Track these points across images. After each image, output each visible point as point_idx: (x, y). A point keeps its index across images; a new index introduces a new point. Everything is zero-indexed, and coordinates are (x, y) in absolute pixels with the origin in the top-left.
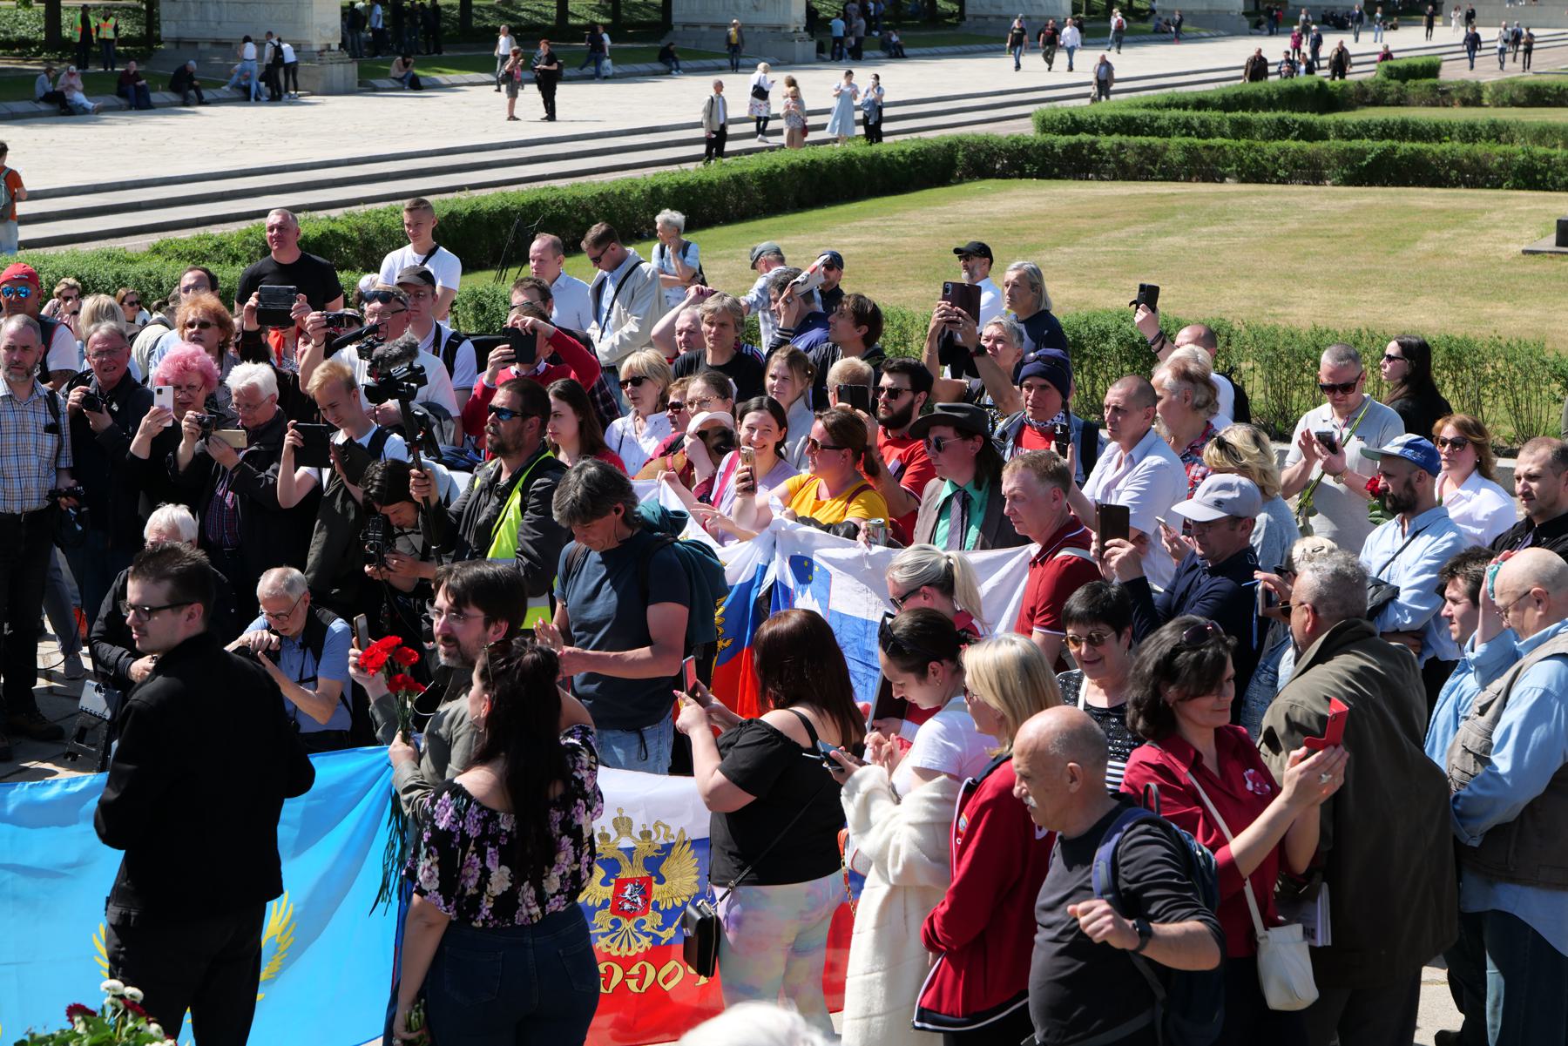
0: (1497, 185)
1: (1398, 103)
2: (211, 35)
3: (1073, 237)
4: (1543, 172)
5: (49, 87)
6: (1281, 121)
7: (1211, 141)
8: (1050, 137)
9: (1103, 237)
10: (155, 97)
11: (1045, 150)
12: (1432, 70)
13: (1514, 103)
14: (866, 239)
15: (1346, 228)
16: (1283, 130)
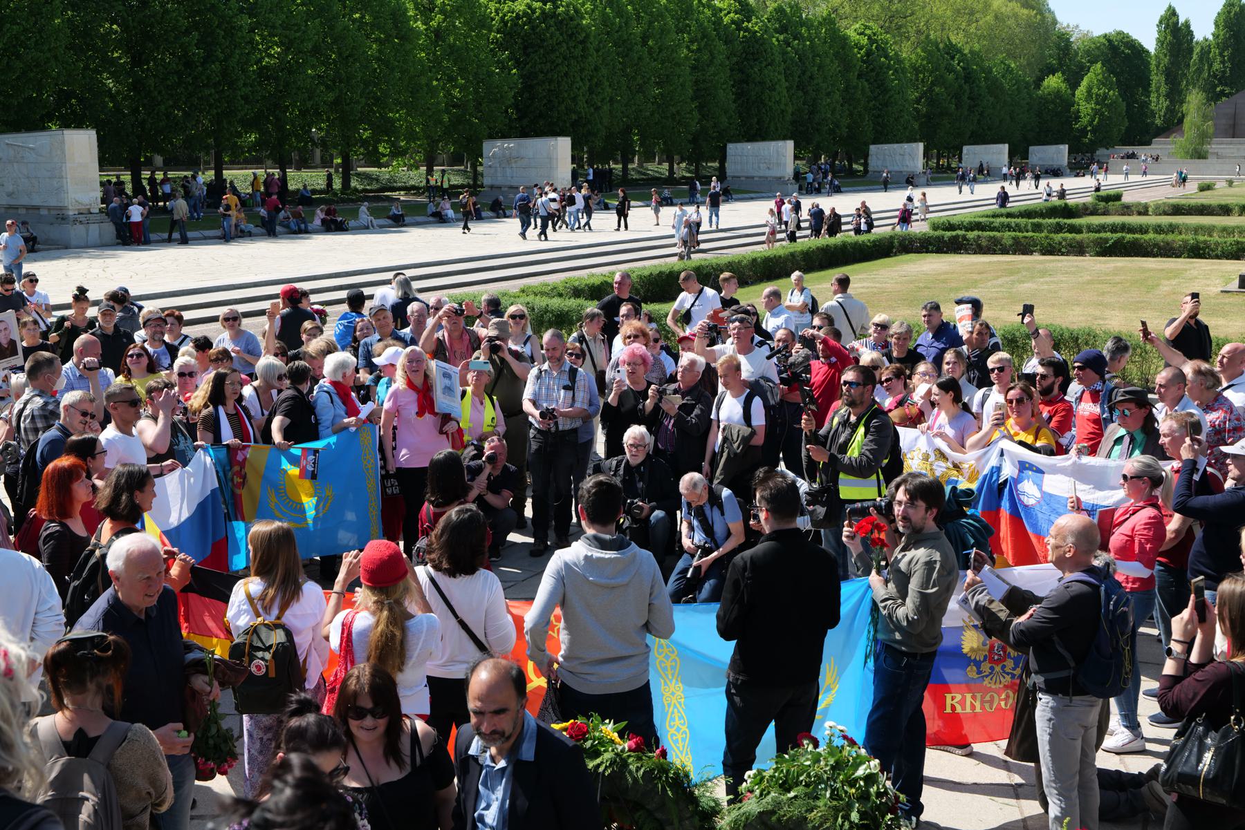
0: (1179, 257)
1: (1104, 214)
2: (508, 183)
4: (1204, 249)
5: (434, 209)
6: (1058, 224)
7: (1026, 234)
8: (939, 233)
9: (989, 284)
10: (484, 214)
11: (940, 239)
12: (1118, 197)
13: (1165, 213)
14: (865, 284)
15: (1117, 279)
16: (1059, 229)
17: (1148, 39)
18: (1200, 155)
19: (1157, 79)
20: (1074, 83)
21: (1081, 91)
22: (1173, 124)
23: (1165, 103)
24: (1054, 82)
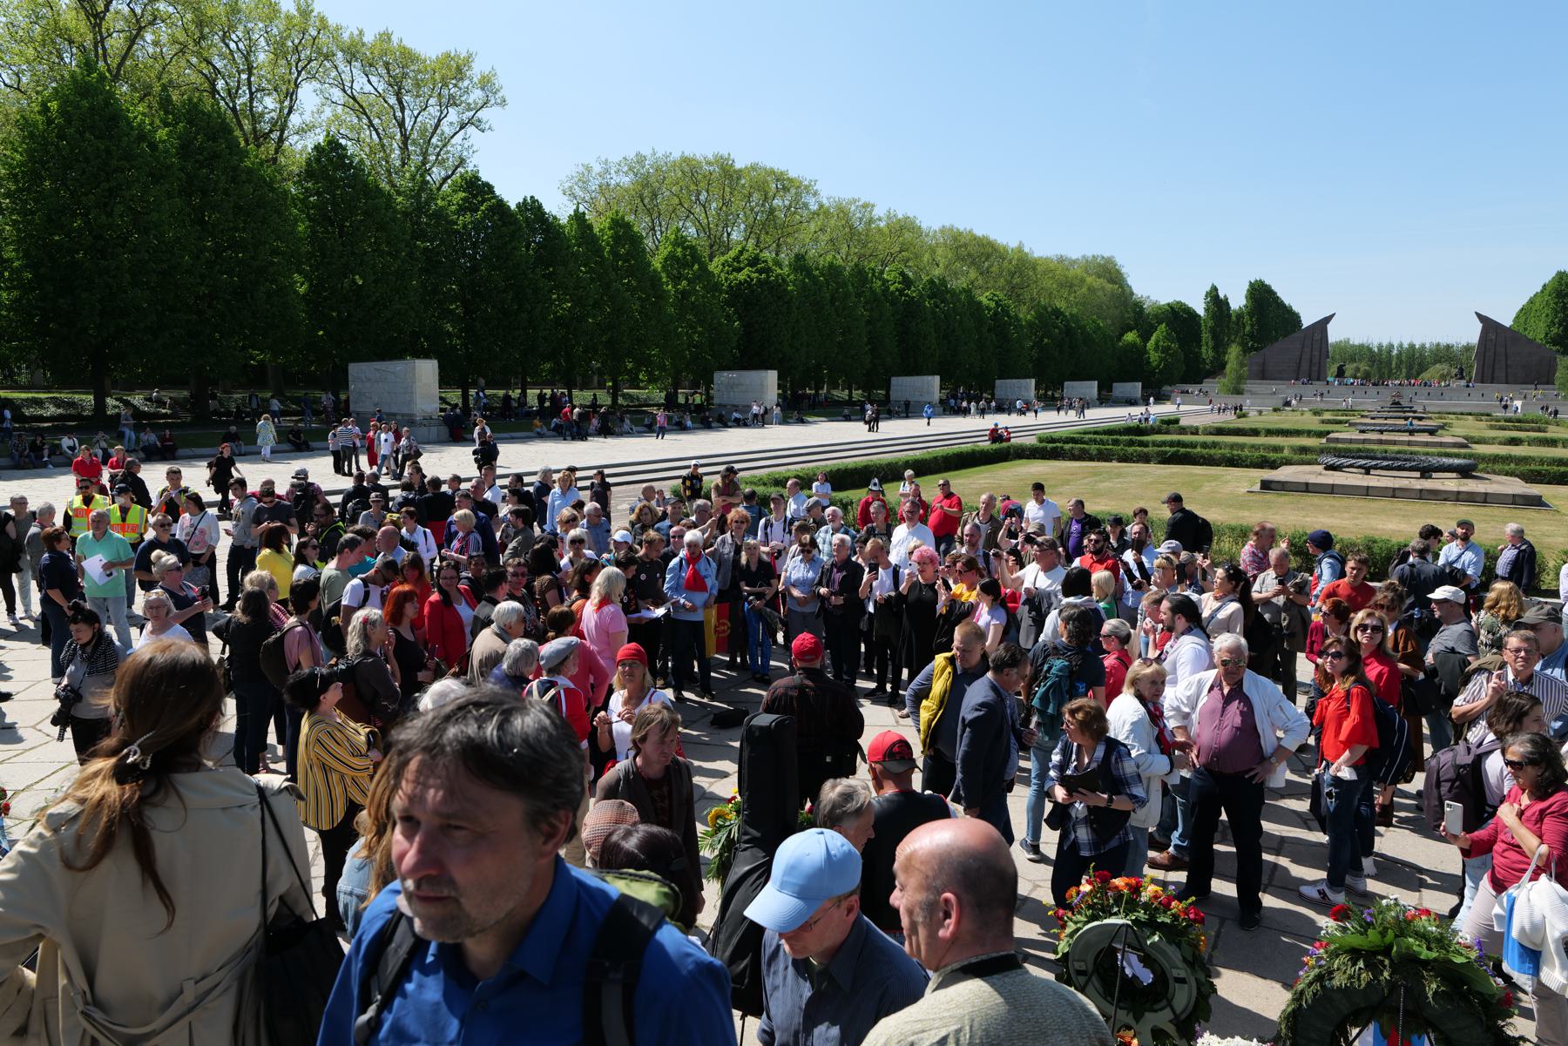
1: (1167, 432)
3: (1067, 482)
11: (1044, 449)
12: (1177, 421)
16: (1131, 443)
17: (1199, 307)
18: (1239, 392)
19: (1206, 336)
20: (1146, 337)
21: (1151, 344)
22: (1218, 369)
23: (1211, 353)
24: (1130, 337)
